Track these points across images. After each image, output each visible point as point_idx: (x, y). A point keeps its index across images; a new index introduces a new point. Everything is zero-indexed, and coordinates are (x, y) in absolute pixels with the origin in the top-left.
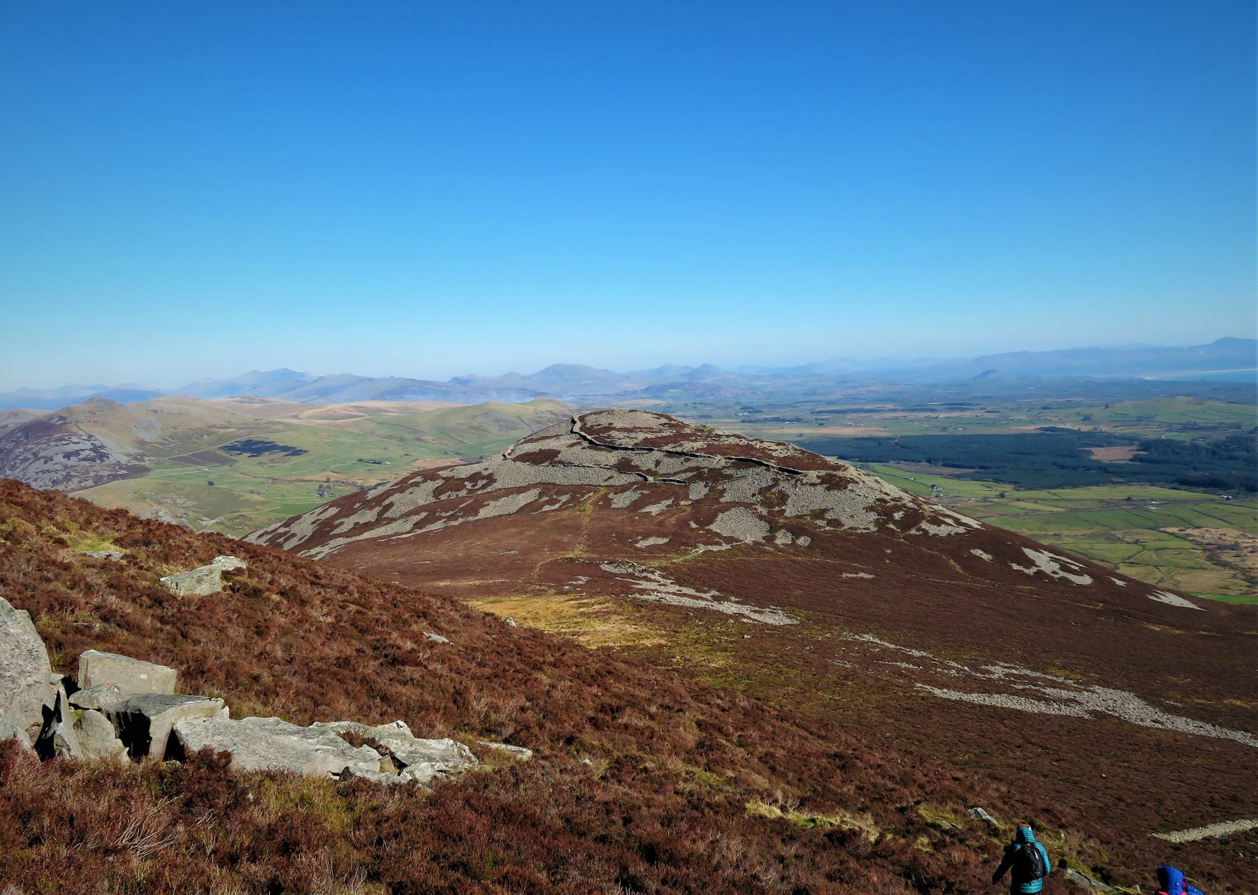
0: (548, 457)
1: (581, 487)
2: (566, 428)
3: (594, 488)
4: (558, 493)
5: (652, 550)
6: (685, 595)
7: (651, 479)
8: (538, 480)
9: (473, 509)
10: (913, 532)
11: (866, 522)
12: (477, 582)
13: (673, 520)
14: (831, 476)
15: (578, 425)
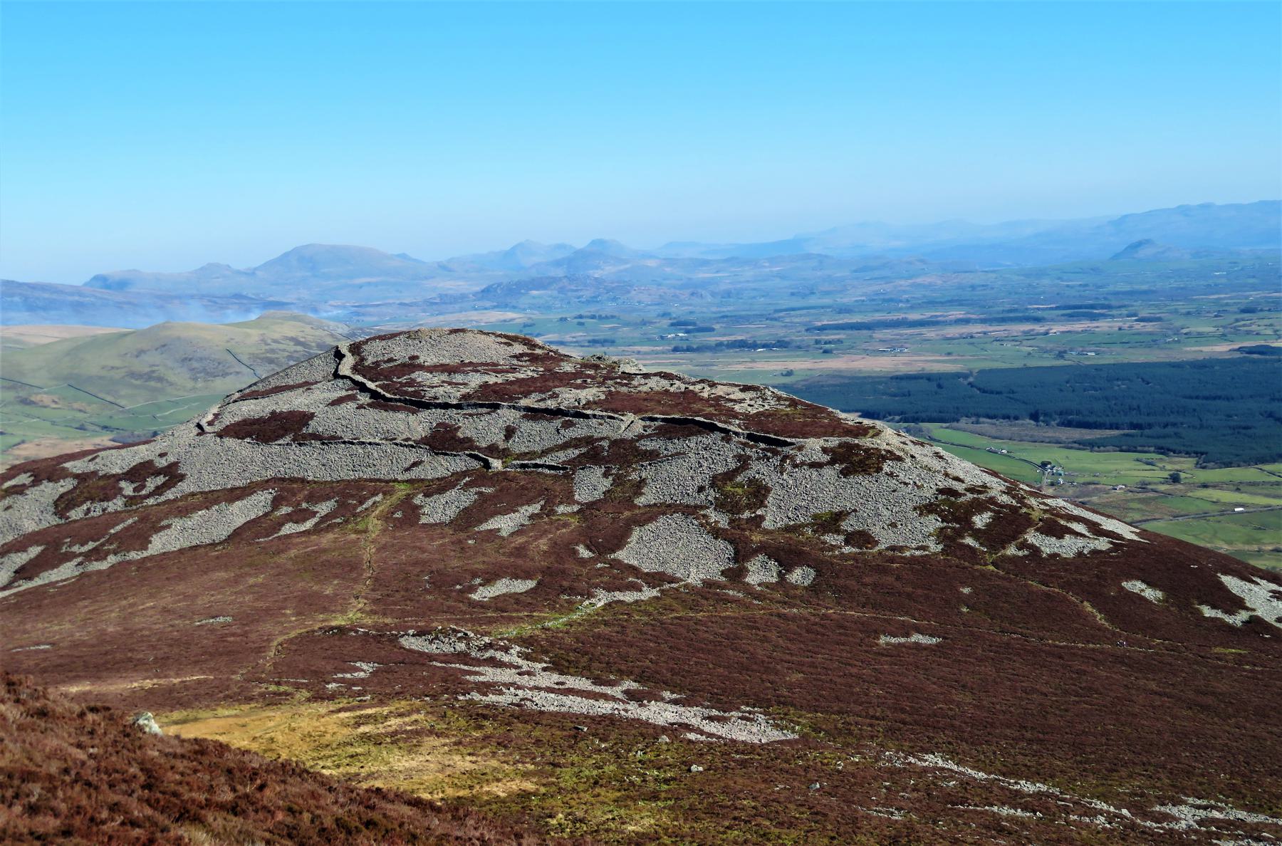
0: (289, 427)
1: (358, 484)
2: (323, 367)
3: (383, 486)
4: (314, 498)
5: (502, 605)
6: (570, 691)
7: (497, 464)
8: (270, 474)
9: (139, 537)
10: (1011, 551)
11: (922, 536)
12: (148, 684)
13: (543, 544)
14: (850, 448)
15: (349, 361)
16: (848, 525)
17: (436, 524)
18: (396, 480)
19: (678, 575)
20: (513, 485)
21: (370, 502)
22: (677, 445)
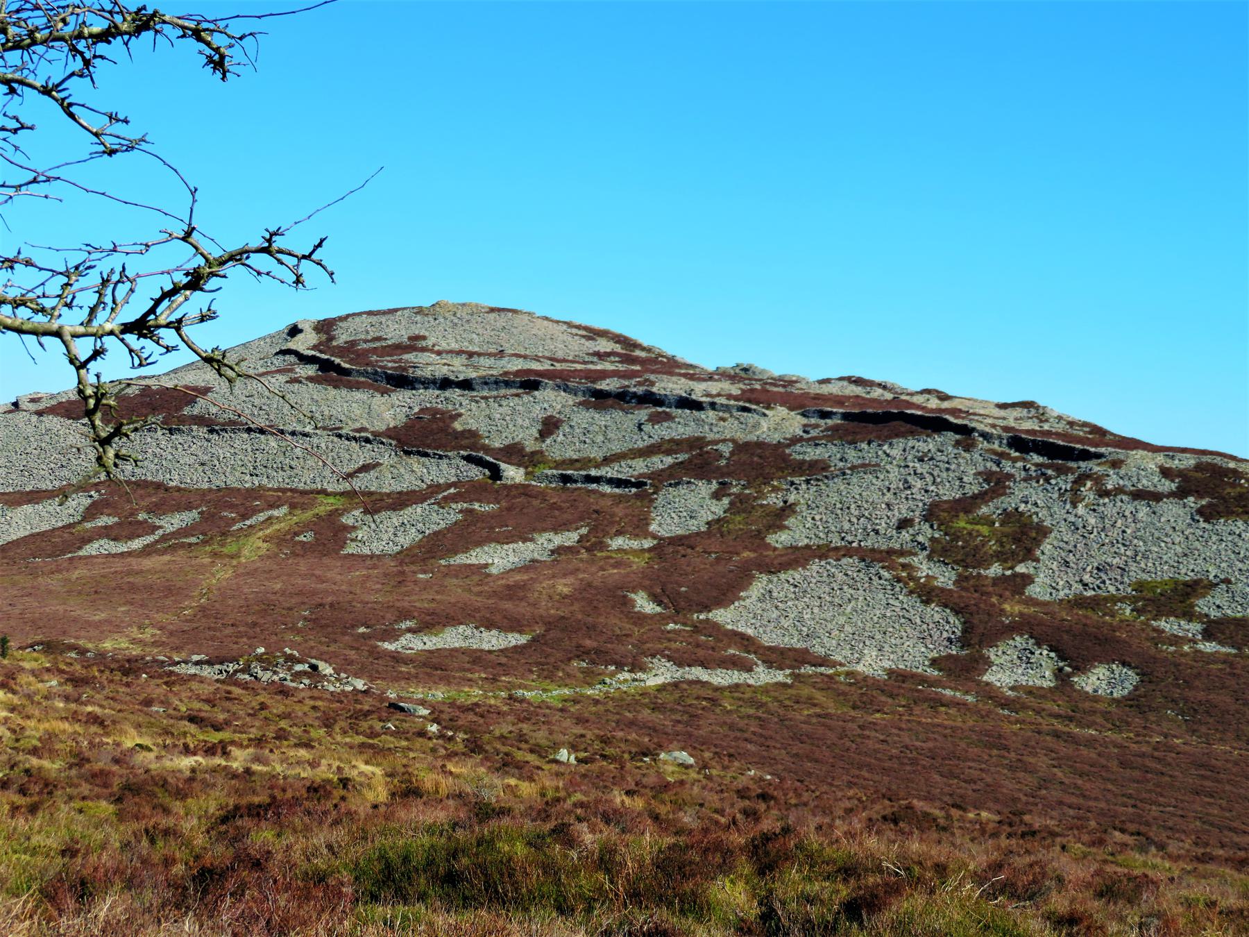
1: (253, 493)
3: (299, 498)
4: (158, 509)
7: (513, 474)
13: (564, 586)
17: (372, 556)
18: (324, 492)
19: (839, 658)
20: (536, 502)
21: (262, 517)
22: (868, 451)
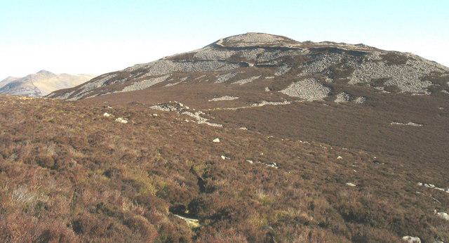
16: (389, 83)
